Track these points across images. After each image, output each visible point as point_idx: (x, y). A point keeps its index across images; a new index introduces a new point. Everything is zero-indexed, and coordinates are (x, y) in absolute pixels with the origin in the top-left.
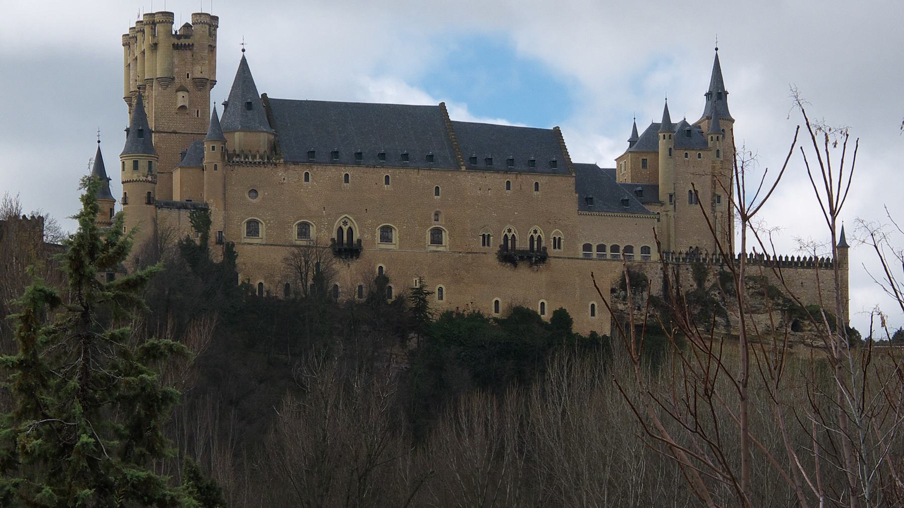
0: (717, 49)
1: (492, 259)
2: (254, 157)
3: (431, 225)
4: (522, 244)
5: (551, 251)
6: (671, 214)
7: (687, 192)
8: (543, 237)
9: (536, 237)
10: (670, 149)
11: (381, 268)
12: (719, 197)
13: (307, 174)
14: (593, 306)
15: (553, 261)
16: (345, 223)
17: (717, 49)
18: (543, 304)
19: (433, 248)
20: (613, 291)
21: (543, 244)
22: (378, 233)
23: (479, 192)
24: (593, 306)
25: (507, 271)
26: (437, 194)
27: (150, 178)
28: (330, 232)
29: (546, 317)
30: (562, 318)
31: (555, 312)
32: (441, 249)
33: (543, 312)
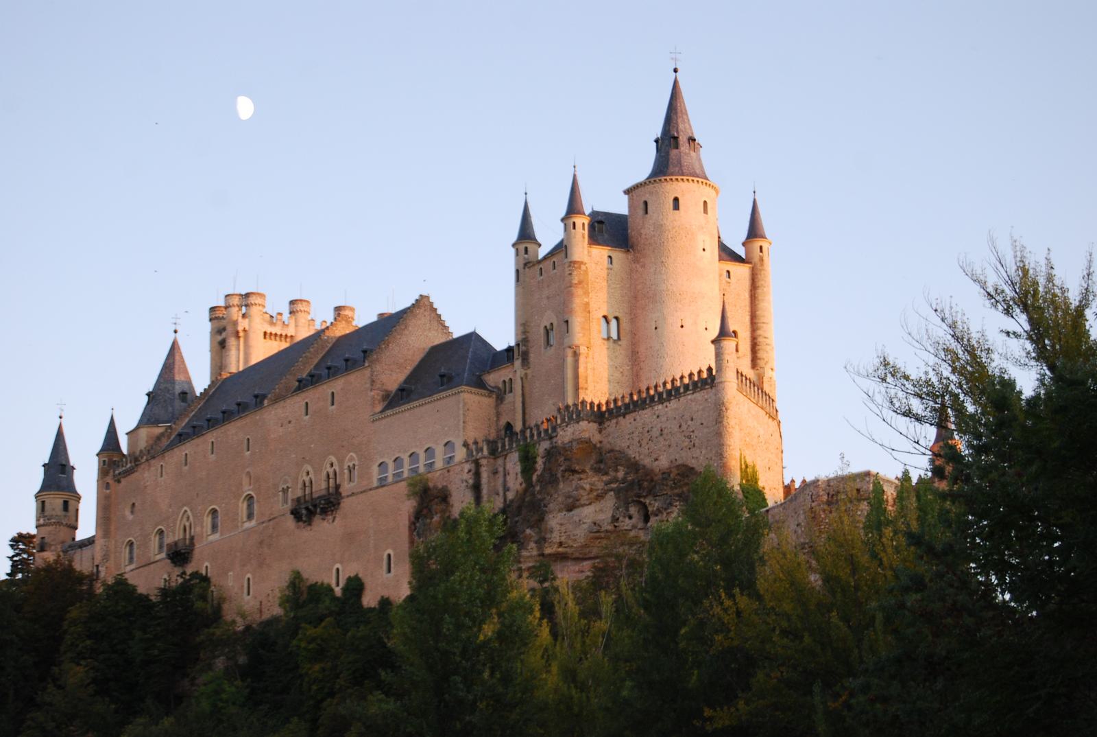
0: (675, 71)
1: (290, 522)
2: (127, 464)
3: (243, 492)
4: (320, 487)
5: (346, 488)
6: (520, 372)
7: (542, 331)
8: (337, 471)
9: (331, 471)
10: (517, 271)
11: (207, 567)
12: (567, 322)
13: (162, 466)
14: (389, 556)
15: (346, 504)
16: (188, 518)
17: (675, 71)
18: (338, 570)
19: (247, 525)
20: (413, 526)
21: (338, 483)
22: (208, 521)
23: (281, 429)
24: (389, 556)
25: (305, 533)
26: (248, 450)
27: (42, 521)
28: (174, 536)
29: (338, 591)
30: (355, 587)
31: (349, 579)
32: (253, 523)
33: (338, 585)
